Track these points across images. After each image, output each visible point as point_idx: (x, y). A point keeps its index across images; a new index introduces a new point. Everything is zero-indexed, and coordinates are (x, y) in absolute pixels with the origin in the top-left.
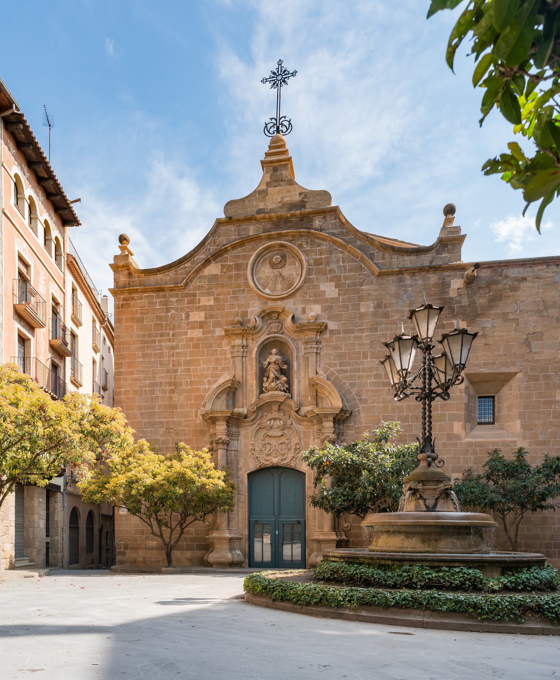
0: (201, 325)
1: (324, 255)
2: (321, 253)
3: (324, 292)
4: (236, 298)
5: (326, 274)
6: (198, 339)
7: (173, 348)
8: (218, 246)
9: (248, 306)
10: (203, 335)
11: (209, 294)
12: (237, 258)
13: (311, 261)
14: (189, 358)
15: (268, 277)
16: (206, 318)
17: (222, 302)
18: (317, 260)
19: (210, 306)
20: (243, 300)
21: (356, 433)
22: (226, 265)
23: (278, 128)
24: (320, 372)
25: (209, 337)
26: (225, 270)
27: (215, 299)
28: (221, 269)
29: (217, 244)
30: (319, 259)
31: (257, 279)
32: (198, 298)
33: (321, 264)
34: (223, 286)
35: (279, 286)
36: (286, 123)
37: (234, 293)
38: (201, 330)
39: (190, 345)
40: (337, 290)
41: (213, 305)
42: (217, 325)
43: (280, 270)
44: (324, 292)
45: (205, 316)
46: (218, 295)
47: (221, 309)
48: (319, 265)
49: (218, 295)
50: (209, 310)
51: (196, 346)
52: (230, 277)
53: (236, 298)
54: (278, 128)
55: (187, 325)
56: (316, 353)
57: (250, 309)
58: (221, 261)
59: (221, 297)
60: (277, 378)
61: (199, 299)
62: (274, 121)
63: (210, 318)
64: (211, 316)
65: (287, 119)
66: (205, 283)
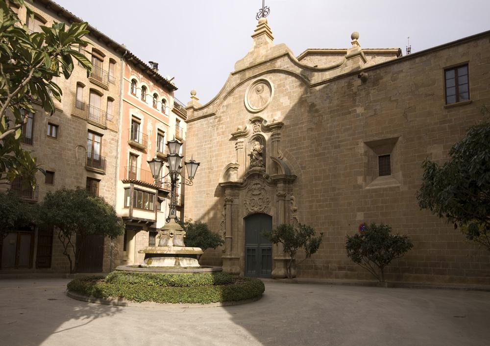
3: (282, 103)
7: (210, 148)
21: (299, 189)
23: (263, 14)
24: (280, 152)
27: (230, 117)
31: (251, 102)
36: (267, 10)
44: (282, 103)
52: (237, 104)
53: (239, 115)
54: (263, 14)
59: (233, 116)
60: (257, 159)
62: (261, 11)
64: (228, 127)
65: (268, 7)
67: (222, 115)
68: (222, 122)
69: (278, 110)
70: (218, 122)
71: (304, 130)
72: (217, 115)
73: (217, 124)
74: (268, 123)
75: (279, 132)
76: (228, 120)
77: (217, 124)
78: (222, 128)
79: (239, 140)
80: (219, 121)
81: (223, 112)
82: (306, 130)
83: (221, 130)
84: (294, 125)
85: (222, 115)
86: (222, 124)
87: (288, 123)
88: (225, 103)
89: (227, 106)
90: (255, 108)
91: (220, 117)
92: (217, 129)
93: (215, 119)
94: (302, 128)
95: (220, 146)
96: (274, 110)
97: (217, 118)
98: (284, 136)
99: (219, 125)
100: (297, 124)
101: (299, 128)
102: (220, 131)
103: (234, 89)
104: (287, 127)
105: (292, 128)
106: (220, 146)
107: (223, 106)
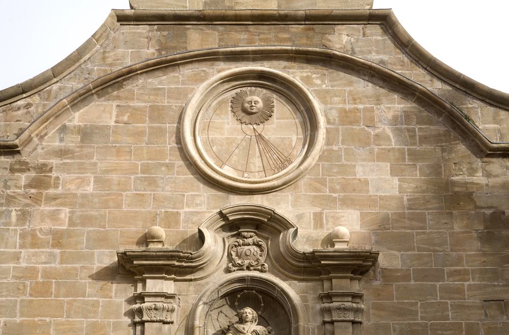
0: (58, 239)
1: (361, 103)
2: (354, 100)
4: (152, 182)
5: (368, 144)
6: (47, 274)
8: (111, 65)
9: (182, 202)
10: (61, 263)
11: (81, 168)
12: (157, 95)
13: (334, 114)
14: (18, 320)
15: (230, 141)
16: (72, 223)
17: (115, 188)
18: (345, 111)
19: (84, 196)
20: (168, 188)
22: (129, 106)
25: (75, 269)
26: (125, 118)
27: (97, 181)
28: (117, 116)
29: (109, 61)
30: (350, 111)
32: (54, 174)
33: (356, 122)
34: (119, 152)
35: (256, 163)
37: (146, 169)
38: (57, 251)
39: (25, 286)
40: (396, 181)
41: (92, 195)
42: (102, 241)
43: (259, 128)
45: (70, 219)
46: (107, 171)
47: (111, 204)
48: (351, 123)
49: (107, 171)
50: (82, 205)
51: (42, 290)
52: (139, 134)
53: (152, 182)
55: (23, 236)
56: (353, 322)
57: (187, 209)
58: (118, 98)
59: (114, 177)
61: (58, 178)
63: (83, 224)
64: (86, 220)
66: (72, 141)
67: (54, 161)
68: (51, 191)
69: (347, 202)
70: (29, 186)
71: (469, 302)
72: (24, 158)
73: (25, 196)
74: (303, 246)
75: (356, 287)
76: (90, 189)
77: (25, 196)
78: (54, 216)
79: (153, 285)
80: (37, 183)
81: (62, 153)
82: (478, 302)
83: (47, 225)
84: (424, 275)
85: (54, 161)
86: (55, 198)
87: (397, 264)
88: (76, 118)
89: (86, 134)
90: (227, 170)
91: (43, 168)
92: (24, 216)
93: (12, 170)
94: (459, 291)
95: (35, 292)
96: (329, 201)
97: (24, 167)
98: (378, 307)
99: (36, 200)
100: (438, 275)
101: (447, 291)
102: (41, 226)
103: (129, 74)
104: (389, 276)
105: (412, 282)
106: (35, 292)
107: (64, 129)
